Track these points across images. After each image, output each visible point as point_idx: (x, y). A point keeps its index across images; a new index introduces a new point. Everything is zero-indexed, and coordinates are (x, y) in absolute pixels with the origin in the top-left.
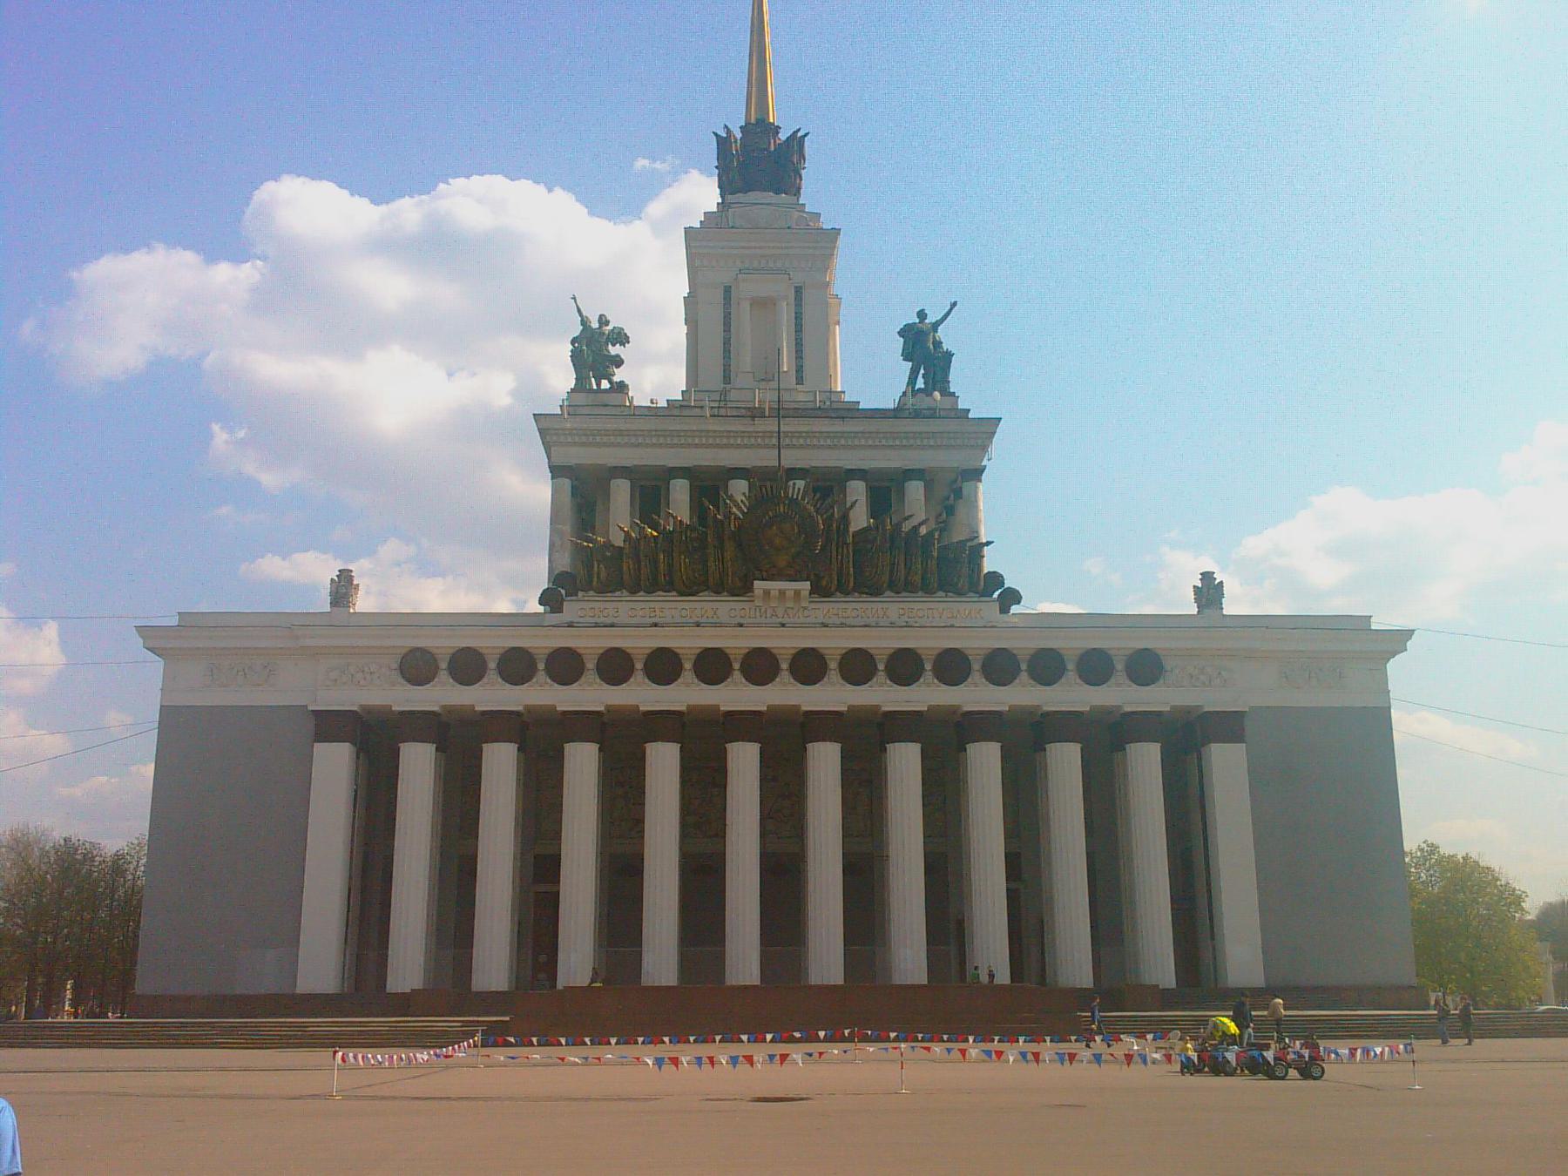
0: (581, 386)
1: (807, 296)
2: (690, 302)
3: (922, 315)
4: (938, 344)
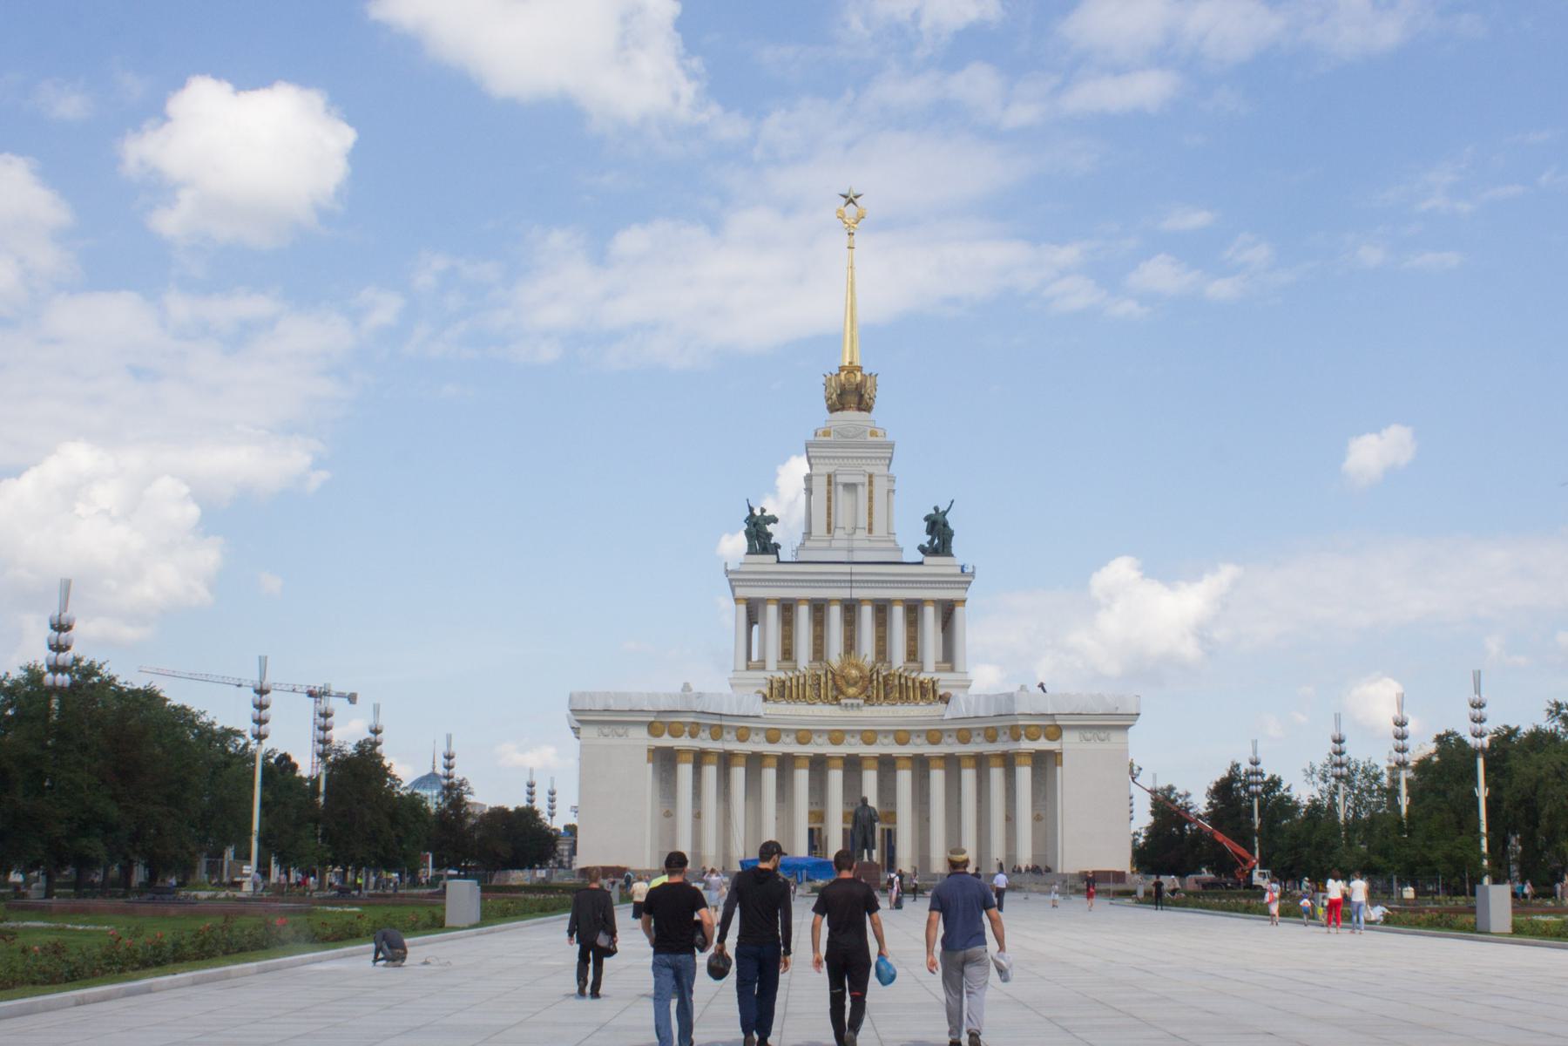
0: (751, 551)
1: (876, 481)
2: (808, 479)
3: (936, 509)
4: (945, 525)
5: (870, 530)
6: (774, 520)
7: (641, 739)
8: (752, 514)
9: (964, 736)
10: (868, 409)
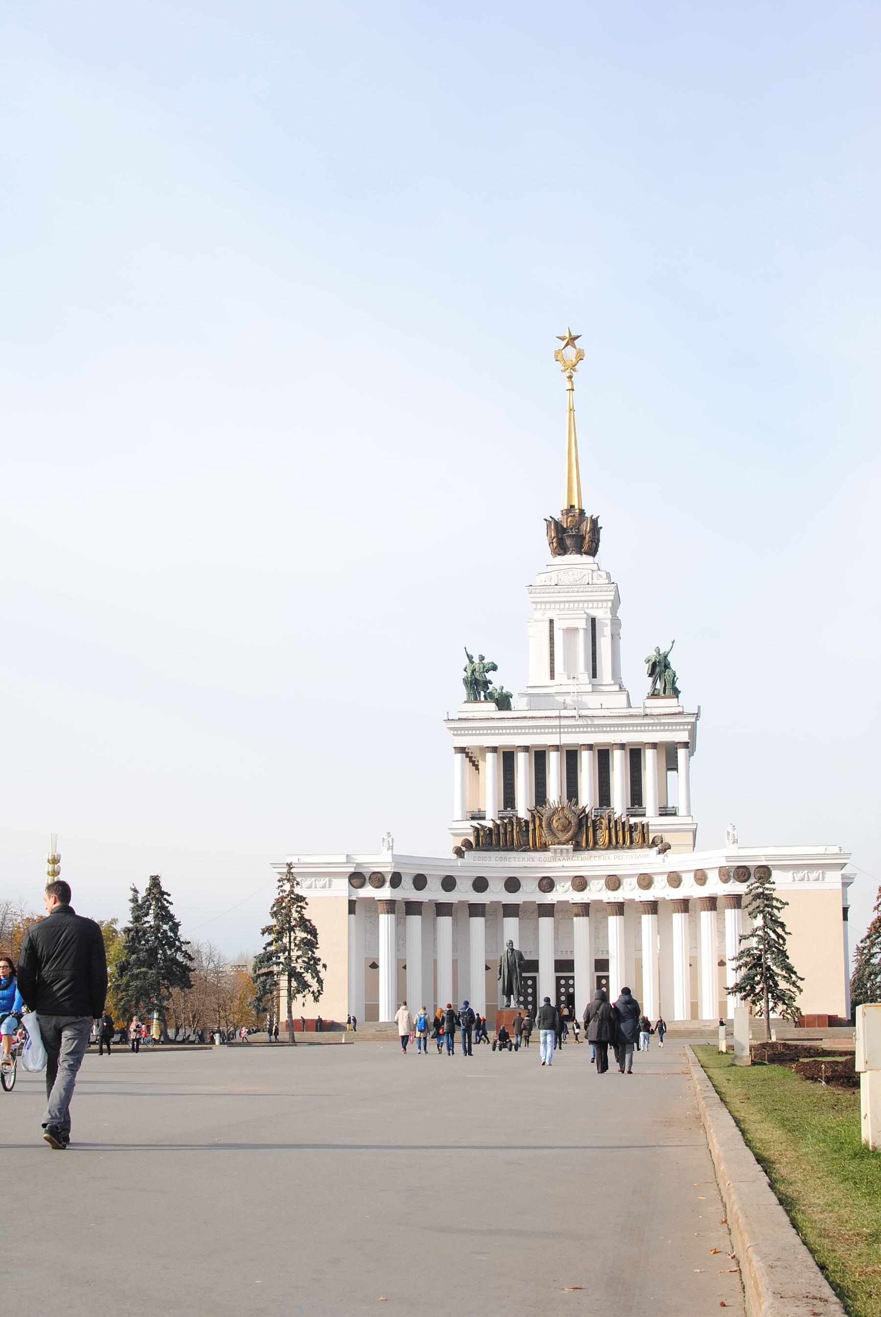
3: (658, 650)
4: (667, 666)
5: (594, 675)
6: (494, 668)
7: (341, 889)
8: (472, 662)
9: (675, 880)
10: (593, 551)
